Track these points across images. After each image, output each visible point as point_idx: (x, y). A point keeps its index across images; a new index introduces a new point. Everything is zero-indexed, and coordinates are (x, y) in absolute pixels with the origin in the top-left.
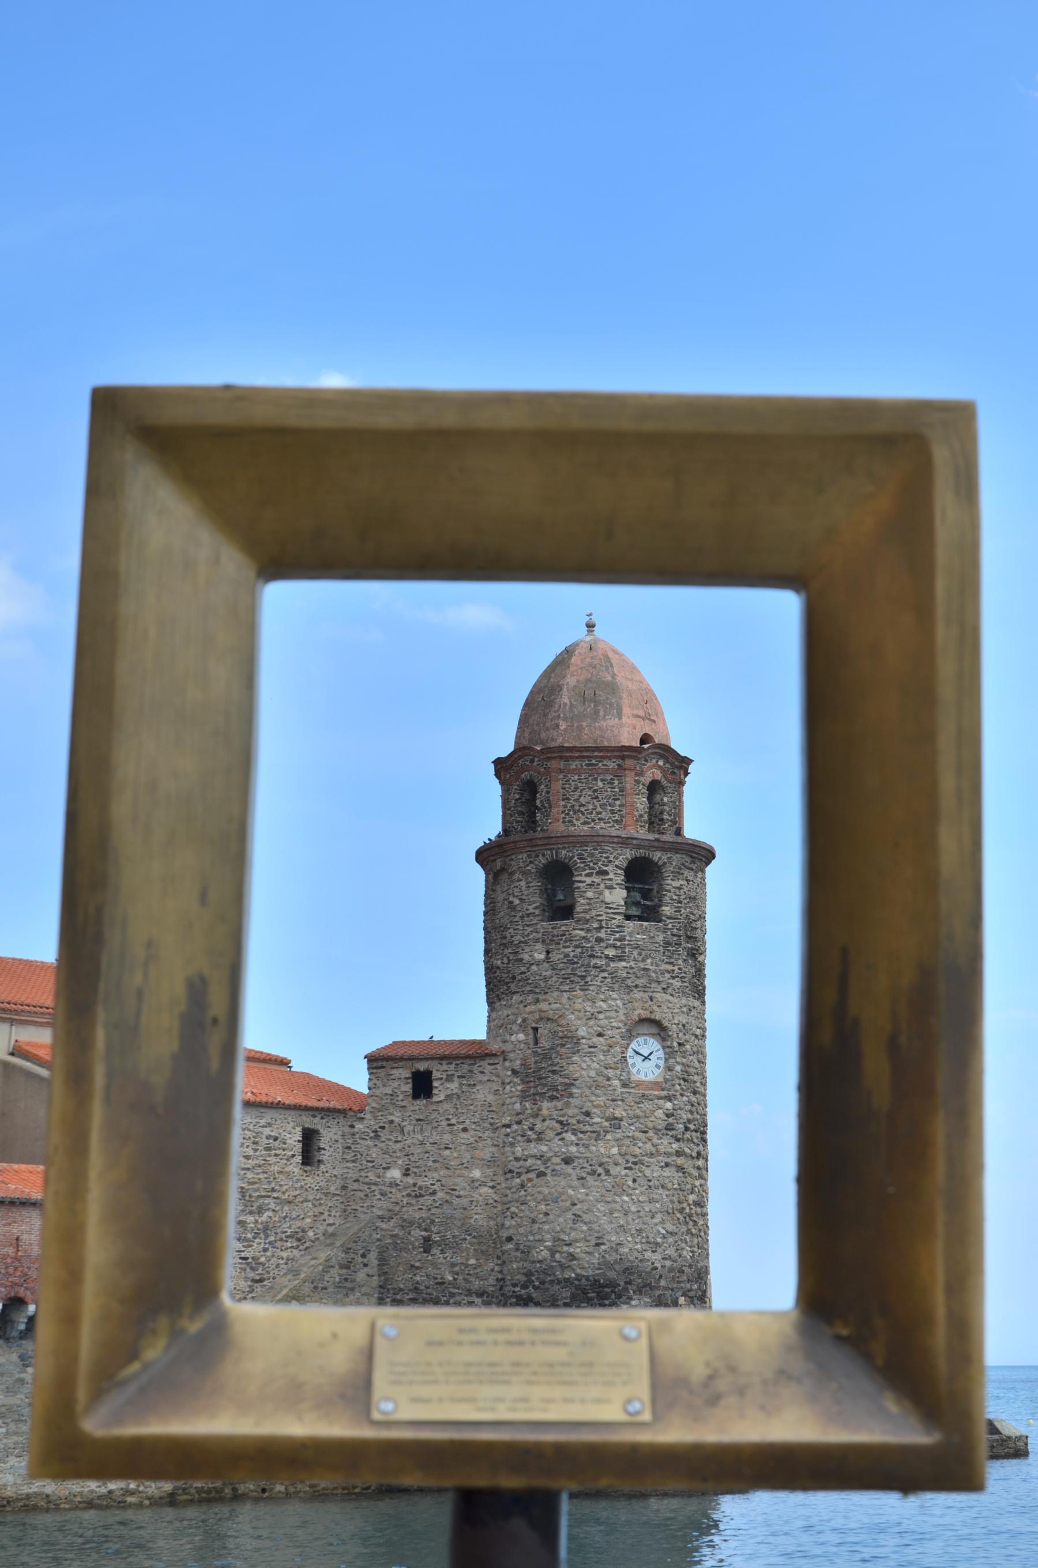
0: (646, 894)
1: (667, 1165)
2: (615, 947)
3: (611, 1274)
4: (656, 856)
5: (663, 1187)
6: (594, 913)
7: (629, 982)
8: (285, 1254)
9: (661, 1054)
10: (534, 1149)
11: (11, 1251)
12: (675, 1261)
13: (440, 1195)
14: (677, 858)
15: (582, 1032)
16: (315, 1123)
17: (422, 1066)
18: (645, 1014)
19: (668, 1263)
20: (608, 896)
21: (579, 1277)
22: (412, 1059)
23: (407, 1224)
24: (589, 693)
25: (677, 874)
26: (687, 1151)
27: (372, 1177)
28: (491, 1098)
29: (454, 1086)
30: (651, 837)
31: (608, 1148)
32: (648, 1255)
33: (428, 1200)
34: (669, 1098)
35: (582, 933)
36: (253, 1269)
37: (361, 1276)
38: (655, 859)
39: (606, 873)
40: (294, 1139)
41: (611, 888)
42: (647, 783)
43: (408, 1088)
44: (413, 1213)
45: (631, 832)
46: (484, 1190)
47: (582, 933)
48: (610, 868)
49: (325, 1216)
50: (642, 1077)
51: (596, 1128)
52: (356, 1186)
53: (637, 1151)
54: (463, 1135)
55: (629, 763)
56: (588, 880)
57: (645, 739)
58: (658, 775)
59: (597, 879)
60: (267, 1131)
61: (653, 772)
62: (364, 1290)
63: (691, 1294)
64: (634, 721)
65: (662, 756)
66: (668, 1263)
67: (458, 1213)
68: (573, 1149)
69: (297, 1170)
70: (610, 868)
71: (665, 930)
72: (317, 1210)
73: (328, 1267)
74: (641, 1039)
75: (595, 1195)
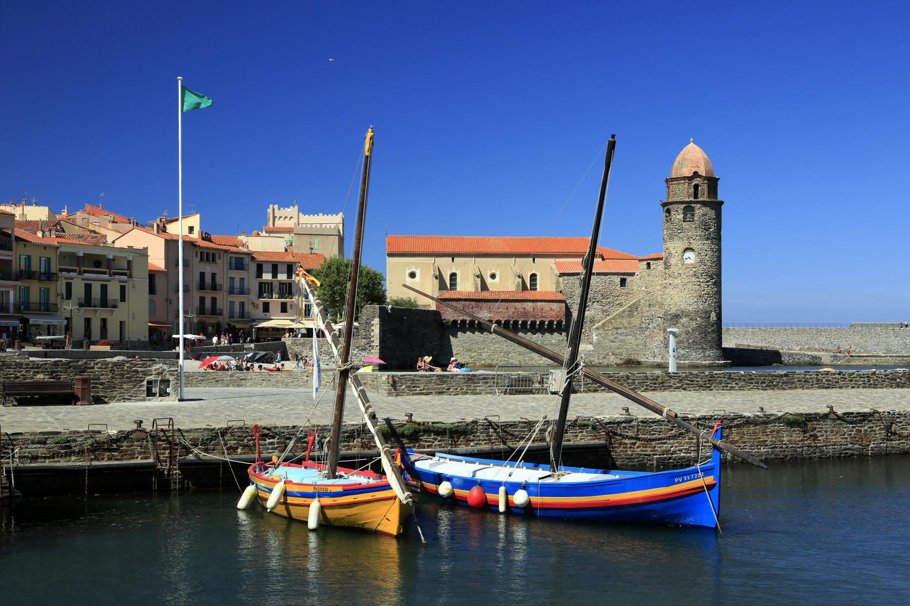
0: (693, 215)
3: (678, 312)
4: (692, 205)
8: (616, 309)
10: (666, 281)
11: (523, 310)
12: (696, 309)
13: (652, 293)
15: (673, 252)
16: (625, 277)
17: (648, 262)
18: (687, 247)
19: (694, 309)
20: (678, 217)
21: (672, 313)
22: (646, 260)
23: (646, 301)
26: (701, 280)
28: (661, 269)
29: (654, 266)
30: (695, 200)
32: (688, 308)
33: (650, 295)
37: (635, 313)
40: (617, 280)
41: (679, 215)
43: (646, 267)
44: (647, 298)
45: (687, 199)
49: (629, 299)
51: (676, 276)
52: (636, 291)
53: (684, 281)
55: (687, 181)
57: (695, 173)
61: (695, 182)
62: (636, 317)
64: (691, 168)
66: (694, 309)
69: (619, 288)
70: (679, 209)
71: (695, 224)
72: (626, 298)
73: (624, 311)
75: (675, 293)
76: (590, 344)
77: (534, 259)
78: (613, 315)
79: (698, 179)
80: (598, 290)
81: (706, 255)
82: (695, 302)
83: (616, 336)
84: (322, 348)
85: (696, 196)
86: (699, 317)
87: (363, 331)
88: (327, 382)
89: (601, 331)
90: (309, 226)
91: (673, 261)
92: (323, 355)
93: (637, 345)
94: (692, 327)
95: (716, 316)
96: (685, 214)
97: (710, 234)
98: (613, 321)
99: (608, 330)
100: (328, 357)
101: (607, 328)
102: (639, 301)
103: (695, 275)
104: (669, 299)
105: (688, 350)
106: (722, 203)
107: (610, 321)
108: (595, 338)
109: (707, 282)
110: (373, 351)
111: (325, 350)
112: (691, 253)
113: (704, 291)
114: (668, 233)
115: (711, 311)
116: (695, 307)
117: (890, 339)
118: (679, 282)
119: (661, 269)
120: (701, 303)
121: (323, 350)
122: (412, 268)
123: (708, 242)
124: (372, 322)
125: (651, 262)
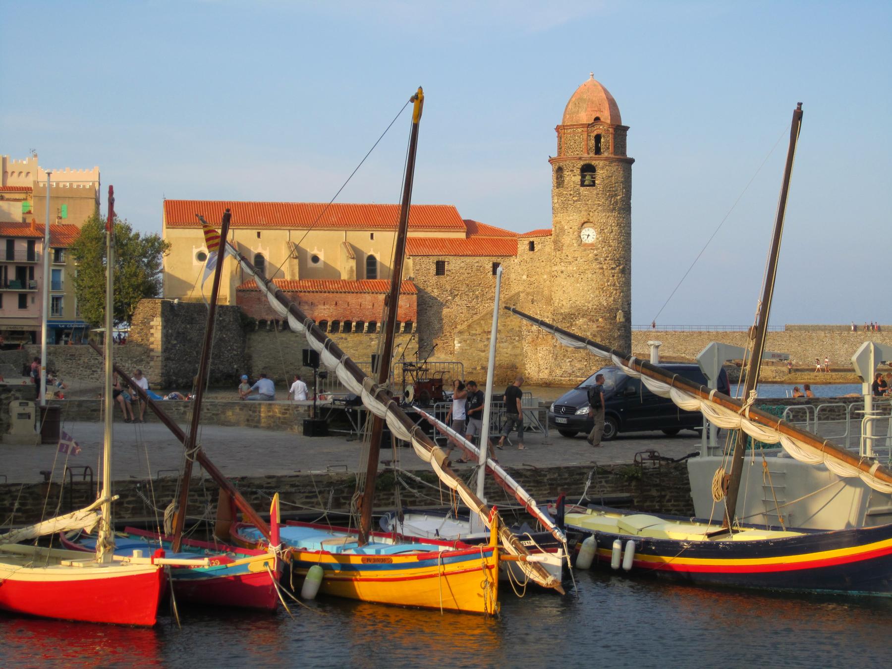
1: (595, 272)
2: (575, 196)
3: (573, 311)
4: (593, 163)
5: (592, 280)
6: (569, 185)
7: (580, 209)
9: (595, 234)
12: (597, 306)
14: (601, 163)
15: (566, 227)
17: (531, 239)
18: (586, 220)
19: (595, 307)
20: (573, 178)
23: (528, 294)
24: (577, 103)
25: (602, 168)
26: (605, 267)
27: (519, 279)
28: (549, 250)
29: (540, 246)
31: (572, 268)
32: (586, 304)
33: (532, 286)
34: (597, 249)
35: (566, 192)
36: (472, 310)
38: (593, 164)
39: (573, 171)
40: (489, 267)
41: (575, 176)
42: (594, 135)
43: (528, 247)
44: (528, 290)
46: (548, 282)
47: (566, 192)
48: (574, 169)
49: (504, 292)
50: (587, 242)
52: (515, 281)
54: (542, 263)
56: (568, 173)
57: (597, 119)
58: (599, 132)
59: (570, 173)
60: (477, 264)
63: (606, 317)
65: (601, 125)
67: (540, 290)
68: (563, 268)
70: (574, 169)
71: (596, 189)
74: (586, 229)
76: (451, 354)
77: (372, 235)
78: (482, 314)
79: (601, 127)
80: (461, 278)
81: (612, 232)
82: (597, 296)
83: (485, 343)
84: (80, 360)
85: (598, 151)
86: (602, 317)
87: (138, 335)
88: (213, 414)
89: (466, 336)
90: (68, 184)
91: (566, 240)
92: (82, 369)
93: (516, 355)
94: (591, 331)
95: (624, 316)
96: (583, 177)
97: (616, 203)
98: (482, 322)
99: (476, 335)
100: (89, 372)
101: (474, 332)
102: (518, 294)
103: (596, 259)
104: (561, 293)
105: (585, 363)
106: (631, 161)
107: (478, 323)
108: (457, 345)
109: (613, 269)
110: (152, 363)
111: (84, 362)
112: (591, 229)
113: (608, 281)
114: (559, 201)
115: (617, 309)
116: (595, 303)
117: (837, 347)
118: (575, 269)
119: (549, 250)
120: (604, 298)
121: (81, 362)
122: (201, 246)
123: (614, 214)
124: (152, 323)
125: (536, 240)
